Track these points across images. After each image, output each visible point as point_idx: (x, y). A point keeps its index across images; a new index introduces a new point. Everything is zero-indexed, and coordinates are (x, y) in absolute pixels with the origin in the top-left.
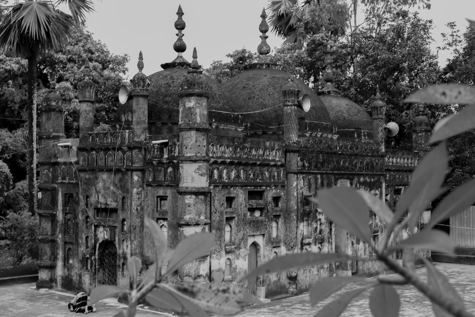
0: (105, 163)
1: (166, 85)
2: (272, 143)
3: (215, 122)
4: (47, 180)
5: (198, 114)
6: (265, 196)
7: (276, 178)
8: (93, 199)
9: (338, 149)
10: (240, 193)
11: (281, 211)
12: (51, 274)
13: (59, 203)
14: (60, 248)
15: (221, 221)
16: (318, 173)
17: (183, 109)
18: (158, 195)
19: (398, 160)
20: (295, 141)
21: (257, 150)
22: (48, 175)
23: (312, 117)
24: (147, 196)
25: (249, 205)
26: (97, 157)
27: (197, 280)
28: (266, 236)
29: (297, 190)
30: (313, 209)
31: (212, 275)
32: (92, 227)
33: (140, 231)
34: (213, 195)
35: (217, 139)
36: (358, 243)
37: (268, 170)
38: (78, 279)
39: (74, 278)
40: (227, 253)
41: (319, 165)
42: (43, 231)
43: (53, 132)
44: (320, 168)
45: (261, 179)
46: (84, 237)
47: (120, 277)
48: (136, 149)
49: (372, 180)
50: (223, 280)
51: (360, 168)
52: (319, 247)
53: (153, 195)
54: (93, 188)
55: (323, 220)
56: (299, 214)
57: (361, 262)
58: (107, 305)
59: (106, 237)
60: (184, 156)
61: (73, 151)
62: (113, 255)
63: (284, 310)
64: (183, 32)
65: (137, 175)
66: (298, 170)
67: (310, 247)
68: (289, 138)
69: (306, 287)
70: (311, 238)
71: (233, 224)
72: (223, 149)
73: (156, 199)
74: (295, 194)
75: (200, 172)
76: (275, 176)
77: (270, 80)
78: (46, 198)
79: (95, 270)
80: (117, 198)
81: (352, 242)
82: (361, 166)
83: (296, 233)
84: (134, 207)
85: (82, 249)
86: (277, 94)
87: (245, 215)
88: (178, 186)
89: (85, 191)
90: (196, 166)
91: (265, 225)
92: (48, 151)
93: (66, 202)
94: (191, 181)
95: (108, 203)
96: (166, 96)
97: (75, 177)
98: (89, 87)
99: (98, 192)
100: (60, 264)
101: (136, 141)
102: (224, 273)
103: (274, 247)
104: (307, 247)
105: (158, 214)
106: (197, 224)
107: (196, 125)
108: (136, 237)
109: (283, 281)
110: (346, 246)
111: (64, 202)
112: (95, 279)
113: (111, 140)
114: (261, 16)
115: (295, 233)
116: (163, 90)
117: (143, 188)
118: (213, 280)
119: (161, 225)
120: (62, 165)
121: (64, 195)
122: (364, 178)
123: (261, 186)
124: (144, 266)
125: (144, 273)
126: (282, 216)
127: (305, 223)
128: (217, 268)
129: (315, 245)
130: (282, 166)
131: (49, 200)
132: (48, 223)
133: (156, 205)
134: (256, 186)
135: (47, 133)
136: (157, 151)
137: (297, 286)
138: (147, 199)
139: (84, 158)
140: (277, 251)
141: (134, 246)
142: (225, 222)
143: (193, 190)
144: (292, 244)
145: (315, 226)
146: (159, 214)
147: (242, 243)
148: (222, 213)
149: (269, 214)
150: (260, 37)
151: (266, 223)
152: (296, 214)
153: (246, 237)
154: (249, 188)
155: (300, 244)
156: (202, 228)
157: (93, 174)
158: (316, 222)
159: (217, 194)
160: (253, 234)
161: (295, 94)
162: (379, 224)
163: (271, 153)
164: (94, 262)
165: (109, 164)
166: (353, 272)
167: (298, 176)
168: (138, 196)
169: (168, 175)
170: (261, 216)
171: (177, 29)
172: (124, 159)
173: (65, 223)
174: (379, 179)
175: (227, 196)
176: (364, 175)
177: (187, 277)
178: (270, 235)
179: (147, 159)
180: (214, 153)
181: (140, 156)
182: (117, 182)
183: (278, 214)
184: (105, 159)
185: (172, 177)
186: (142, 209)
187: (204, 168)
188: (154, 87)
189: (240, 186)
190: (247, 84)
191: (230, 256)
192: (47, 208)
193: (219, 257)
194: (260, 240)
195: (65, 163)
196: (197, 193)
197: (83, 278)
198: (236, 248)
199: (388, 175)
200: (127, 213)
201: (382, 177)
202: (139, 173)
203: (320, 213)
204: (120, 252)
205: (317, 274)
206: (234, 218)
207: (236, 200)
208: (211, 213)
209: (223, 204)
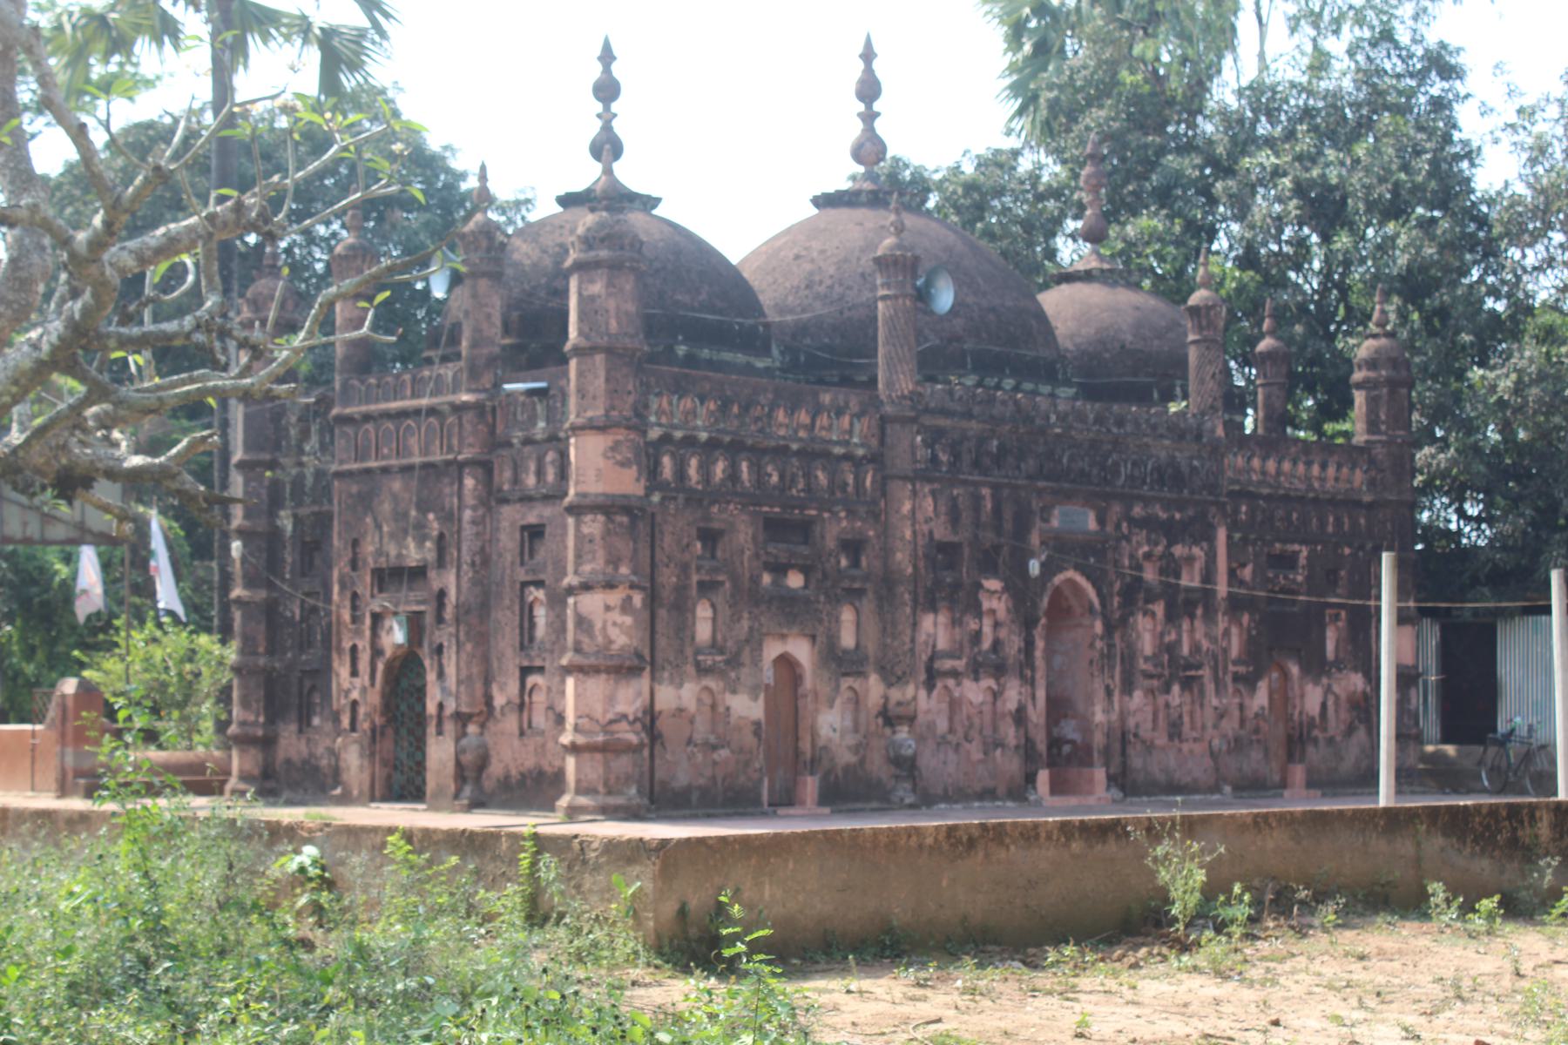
3: (682, 343)
5: (612, 313)
7: (850, 489)
8: (369, 548)
9: (1053, 418)
11: (866, 578)
16: (984, 484)
18: (524, 522)
19: (1286, 466)
21: (792, 411)
23: (984, 335)
25: (767, 553)
28: (819, 639)
31: (658, 723)
34: (659, 519)
36: (1128, 687)
37: (824, 469)
39: (324, 762)
40: (702, 671)
41: (987, 461)
49: (1178, 516)
50: (690, 741)
51: (1131, 478)
54: (368, 520)
57: (1139, 746)
64: (615, 107)
65: (475, 478)
66: (915, 471)
67: (959, 684)
69: (946, 790)
70: (959, 658)
71: (720, 598)
72: (687, 403)
73: (518, 536)
74: (908, 534)
75: (619, 457)
76: (846, 484)
82: (1136, 473)
83: (913, 640)
84: (466, 558)
87: (756, 580)
103: (846, 674)
104: (951, 682)
106: (610, 586)
110: (1090, 701)
115: (907, 639)
117: (489, 509)
118: (660, 736)
122: (1146, 506)
123: (802, 508)
126: (870, 595)
127: (943, 618)
128: (674, 706)
129: (977, 679)
133: (518, 550)
137: (915, 785)
140: (856, 686)
142: (694, 592)
143: (600, 500)
145: (973, 625)
146: (527, 572)
148: (684, 569)
149: (829, 583)
150: (859, 115)
151: (820, 607)
152: (911, 588)
154: (766, 509)
156: (623, 595)
158: (979, 614)
162: (1205, 644)
166: (1112, 771)
168: (475, 529)
170: (806, 587)
171: (598, 98)
175: (702, 525)
176: (1147, 501)
180: (664, 412)
183: (857, 585)
190: (806, 249)
194: (801, 650)
196: (608, 507)
198: (727, 662)
199: (1244, 508)
201: (1213, 510)
202: (480, 471)
205: (980, 761)
206: (722, 583)
208: (653, 565)
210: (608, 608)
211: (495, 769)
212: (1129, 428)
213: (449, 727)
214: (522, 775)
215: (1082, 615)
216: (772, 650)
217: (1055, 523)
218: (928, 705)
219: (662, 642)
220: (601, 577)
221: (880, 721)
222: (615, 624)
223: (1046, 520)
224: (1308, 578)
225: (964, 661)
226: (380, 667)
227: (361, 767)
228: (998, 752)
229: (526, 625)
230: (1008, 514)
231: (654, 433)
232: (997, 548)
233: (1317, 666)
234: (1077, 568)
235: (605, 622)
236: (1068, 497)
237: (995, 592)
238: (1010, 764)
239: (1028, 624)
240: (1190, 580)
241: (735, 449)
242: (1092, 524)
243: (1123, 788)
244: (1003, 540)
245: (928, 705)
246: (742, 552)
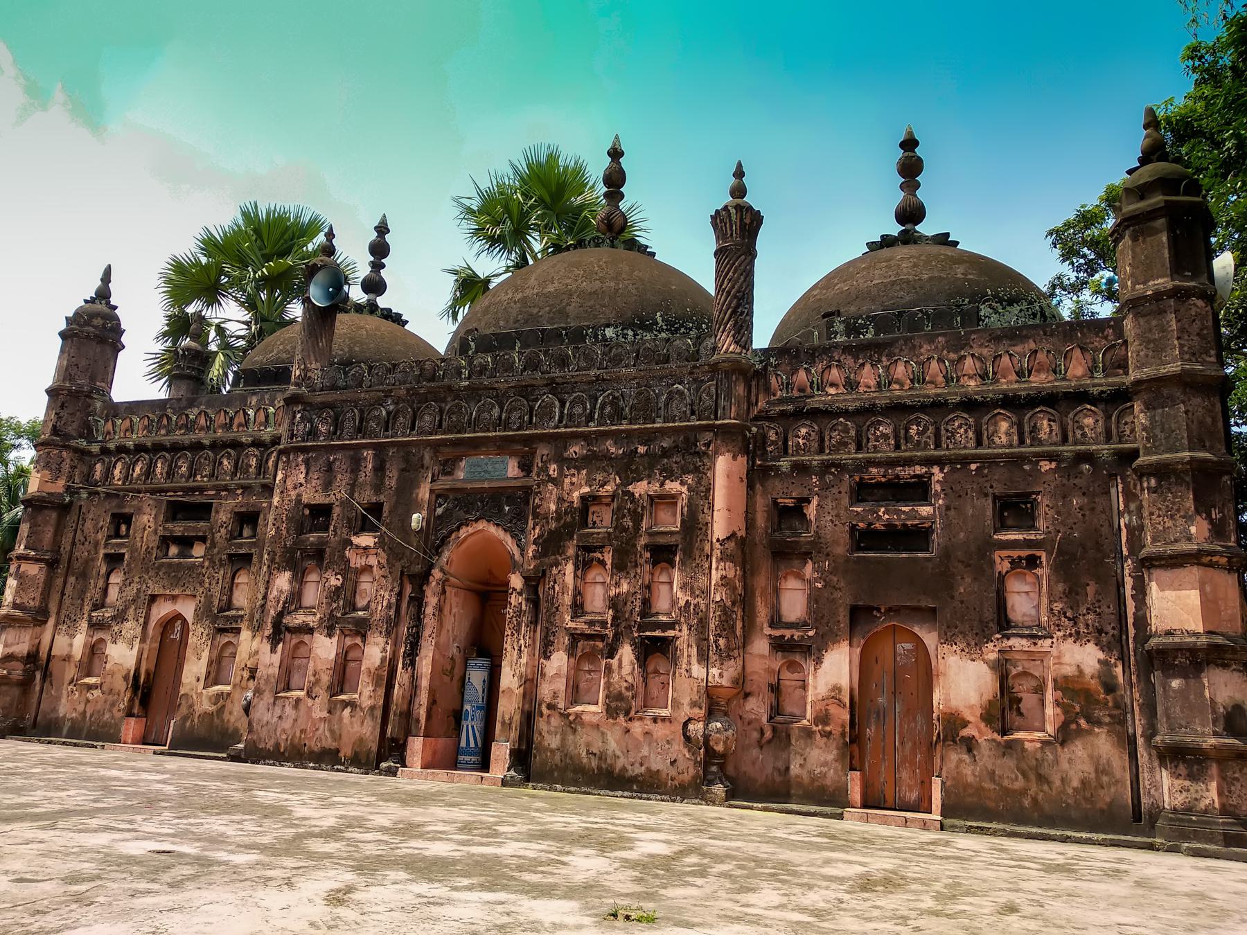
15: (93, 560)
16: (366, 446)
34: (84, 510)
45: (206, 476)
51: (570, 416)
69: (277, 745)
76: (251, 466)
83: (265, 597)
109: (232, 719)
115: (260, 597)
134: (190, 491)
147: (132, 610)
149: (216, 550)
151: (204, 571)
155: (270, 625)
159: (93, 508)
198: (114, 618)
201: (709, 436)
203: (358, 547)
205: (324, 719)
208: (73, 544)
209: (102, 528)
216: (162, 610)
217: (461, 475)
225: (318, 616)
228: (347, 711)
240: (670, 522)
244: (382, 498)
246: (144, 529)
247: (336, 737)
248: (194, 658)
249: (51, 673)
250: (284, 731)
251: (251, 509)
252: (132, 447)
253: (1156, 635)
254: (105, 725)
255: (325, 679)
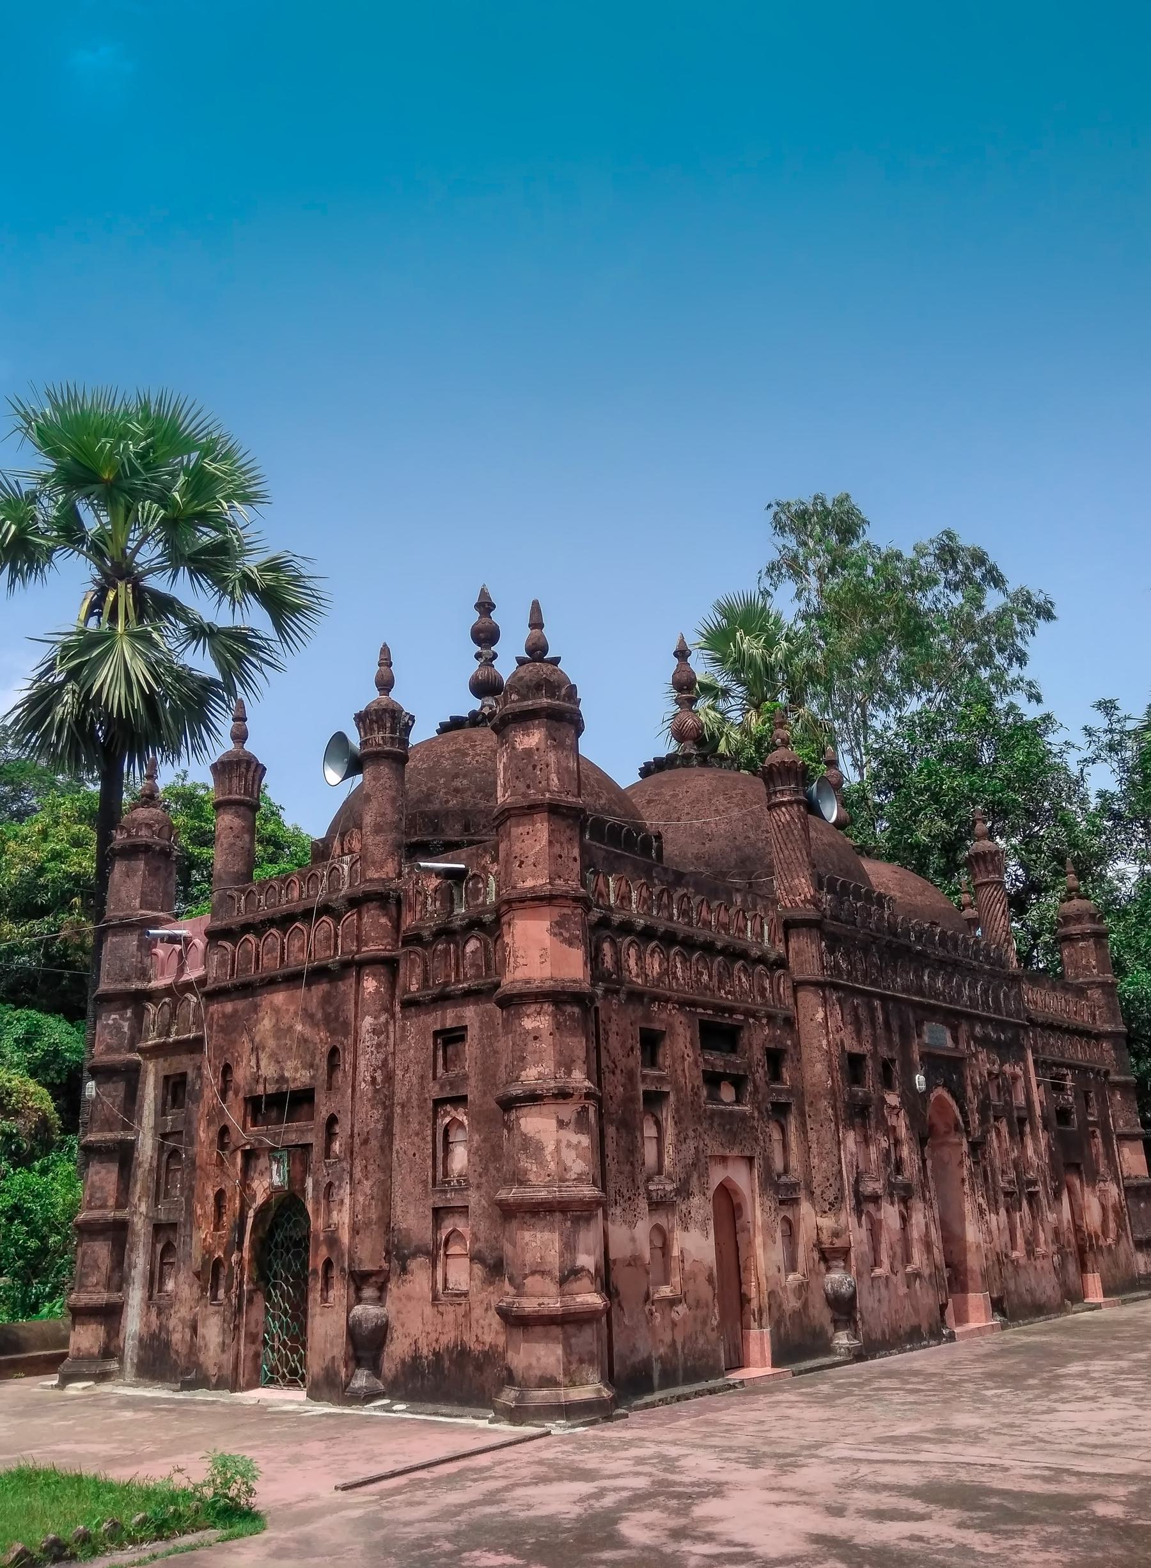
0: (282, 959)
1: (453, 754)
2: (749, 899)
4: (113, 1042)
6: (745, 1041)
7: (768, 994)
8: (241, 1075)
10: (677, 1024)
11: (789, 1092)
12: (108, 1333)
13: (146, 1107)
14: (141, 1246)
15: (632, 1100)
17: (510, 758)
20: (809, 897)
22: (118, 1028)
24: (403, 1038)
26: (257, 946)
27: (567, 1287)
29: (827, 1033)
30: (874, 1096)
31: (613, 1278)
32: (235, 1159)
33: (382, 1148)
35: (605, 858)
37: (745, 970)
38: (188, 1338)
39: (176, 1337)
42: (91, 1196)
43: (141, 908)
44: (876, 979)
46: (211, 1193)
47: (318, 1310)
48: (371, 900)
49: (1003, 1037)
50: (647, 1297)
52: (900, 1212)
53: (421, 1032)
54: (245, 1038)
55: (903, 1132)
56: (838, 1105)
58: (270, 1409)
59: (277, 1180)
60: (514, 888)
61: (193, 950)
62: (297, 1244)
63: (850, 1394)
65: (374, 976)
67: (879, 1209)
68: (790, 890)
69: (883, 1333)
73: (430, 1042)
74: (824, 1042)
75: (566, 935)
76: (765, 989)
77: (714, 782)
78: (109, 1096)
79: (240, 1297)
80: (313, 1056)
81: (980, 1205)
83: (840, 1162)
84: (364, 1073)
85: (203, 1234)
86: (737, 809)
88: (498, 985)
89: (220, 1050)
90: (555, 912)
91: (753, 1127)
92: (122, 960)
93: (164, 1104)
94: (538, 960)
95: (287, 1074)
96: (456, 776)
97: (194, 1023)
98: (244, 765)
99: (255, 1050)
100: (136, 1296)
101: (371, 880)
102: (648, 1273)
103: (782, 1202)
104: (871, 1207)
105: (437, 1088)
106: (563, 1095)
107: (547, 795)
108: (370, 1168)
111: (160, 1102)
112: (237, 1328)
113: (301, 892)
114: (676, 654)
116: (446, 764)
117: (393, 1016)
118: (618, 1294)
119: (447, 1120)
120: (162, 998)
121: (161, 1080)
124: (395, 1262)
125: (394, 1290)
126: (793, 1108)
130: (781, 963)
131: (118, 1101)
132: (109, 1172)
134: (720, 1009)
135: (123, 910)
136: (434, 900)
138: (403, 1047)
139: (222, 956)
140: (790, 1216)
141: (361, 1199)
144: (830, 1195)
145: (885, 1145)
146: (442, 1087)
148: (630, 1075)
149: (760, 1097)
153: (703, 1160)
154: (700, 1010)
156: (578, 1107)
157: (246, 997)
159: (614, 1016)
160: (720, 1151)
161: (796, 773)
163: (749, 923)
164: (237, 1270)
165: (292, 959)
166: (995, 1296)
167: (827, 992)
169: (467, 962)
170: (738, 1101)
172: (336, 935)
173: (158, 1166)
174: (1017, 1036)
175: (644, 1025)
177: (538, 1277)
178: (768, 1161)
179: (403, 928)
180: (601, 895)
181: (383, 920)
182: (314, 1005)
183: (783, 1100)
184: (283, 948)
185: (479, 967)
186: (389, 1078)
187: (575, 923)
188: (421, 760)
189: (676, 1002)
191: (662, 1221)
192: (108, 1125)
193: (629, 1218)
195: (168, 991)
197: (200, 1330)
198: (678, 1192)
200: (343, 1096)
201: (1022, 1032)
202: (382, 969)
203: (890, 1107)
204: (317, 1224)
205: (906, 1295)
207: (668, 1042)
209: (632, 1049)
210: (561, 1124)
211: (397, 1349)
212: (961, 948)
213: (339, 1292)
214: (436, 1354)
215: (947, 1133)
216: (717, 1176)
217: (926, 1039)
218: (857, 1235)
219: (612, 1167)
220: (552, 1084)
221: (816, 1255)
222: (569, 1145)
223: (919, 1036)
224: (1075, 1098)
226: (251, 1213)
227: (223, 1347)
229: (440, 1154)
230: (895, 1024)
231: (595, 915)
232: (893, 1061)
233: (1092, 1178)
234: (944, 1086)
235: (558, 1142)
236: (931, 1012)
237: (895, 1107)
238: (927, 1298)
239: (922, 1142)
241: (669, 939)
242: (950, 1043)
243: (1003, 1313)
245: (857, 1235)
247: (916, 1311)
248: (770, 1242)
249: (616, 1290)
250: (884, 1314)
251: (779, 1046)
252: (639, 929)
253: (1129, 1178)
254: (703, 1355)
255: (899, 1250)
